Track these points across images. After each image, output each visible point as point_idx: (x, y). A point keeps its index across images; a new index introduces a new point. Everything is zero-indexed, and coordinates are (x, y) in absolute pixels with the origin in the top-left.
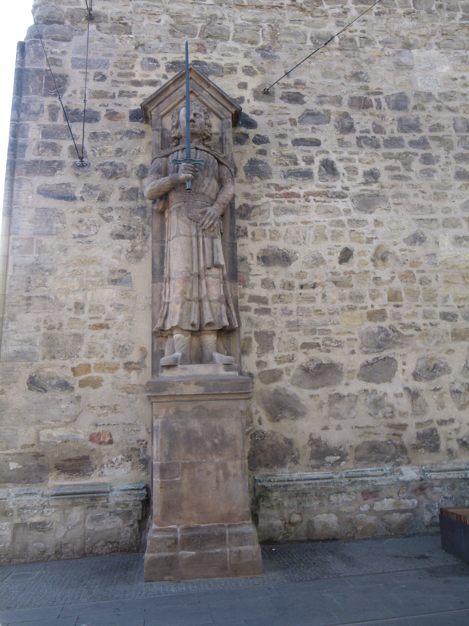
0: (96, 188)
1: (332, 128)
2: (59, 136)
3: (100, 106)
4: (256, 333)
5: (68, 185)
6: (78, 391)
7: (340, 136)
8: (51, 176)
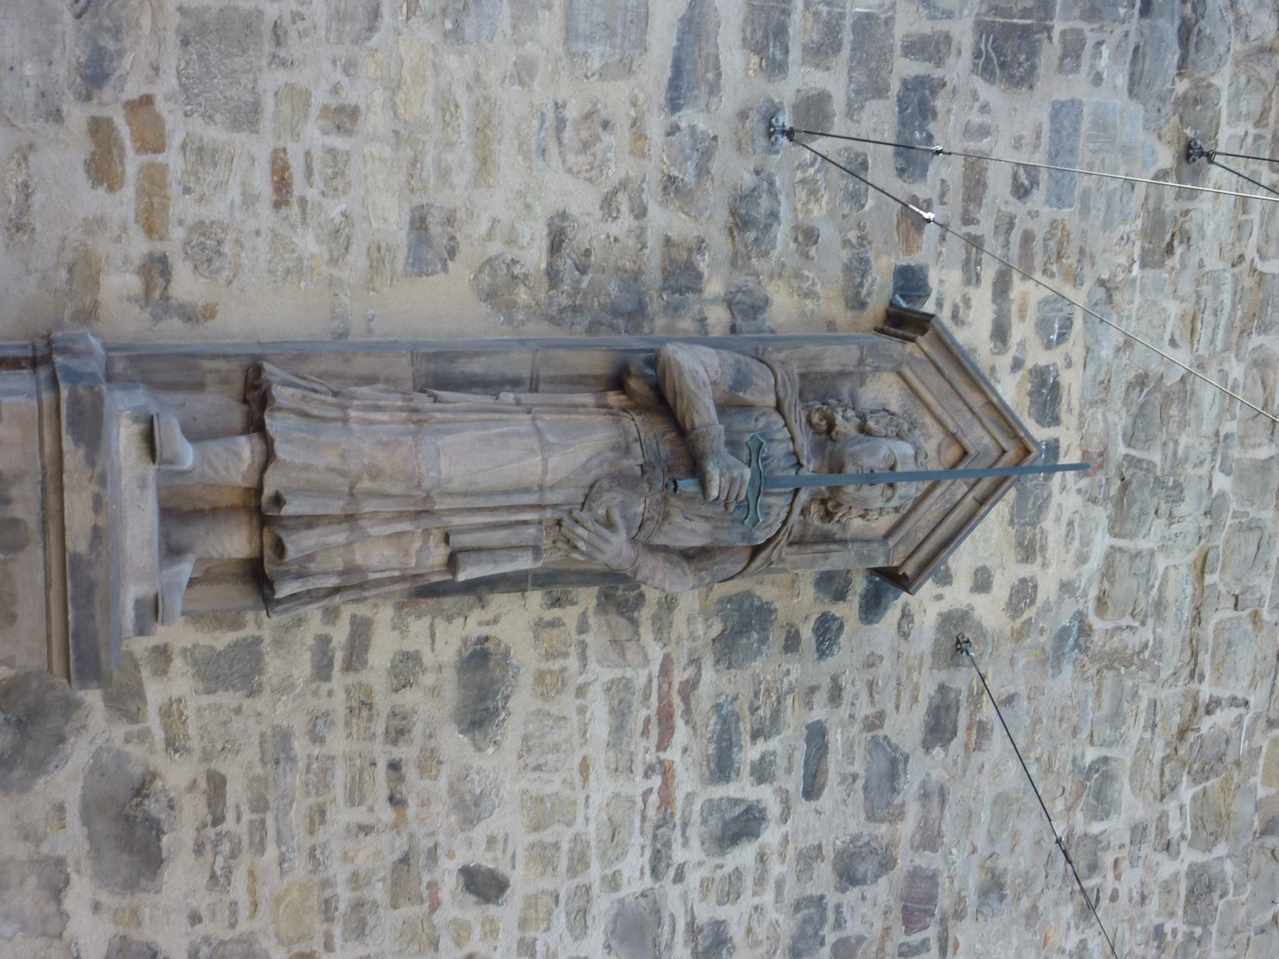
0: (703, 171)
1: (853, 828)
2: (859, 63)
3: (943, 181)
4: (257, 641)
5: (714, 89)
6: (77, 115)
8: (744, 39)
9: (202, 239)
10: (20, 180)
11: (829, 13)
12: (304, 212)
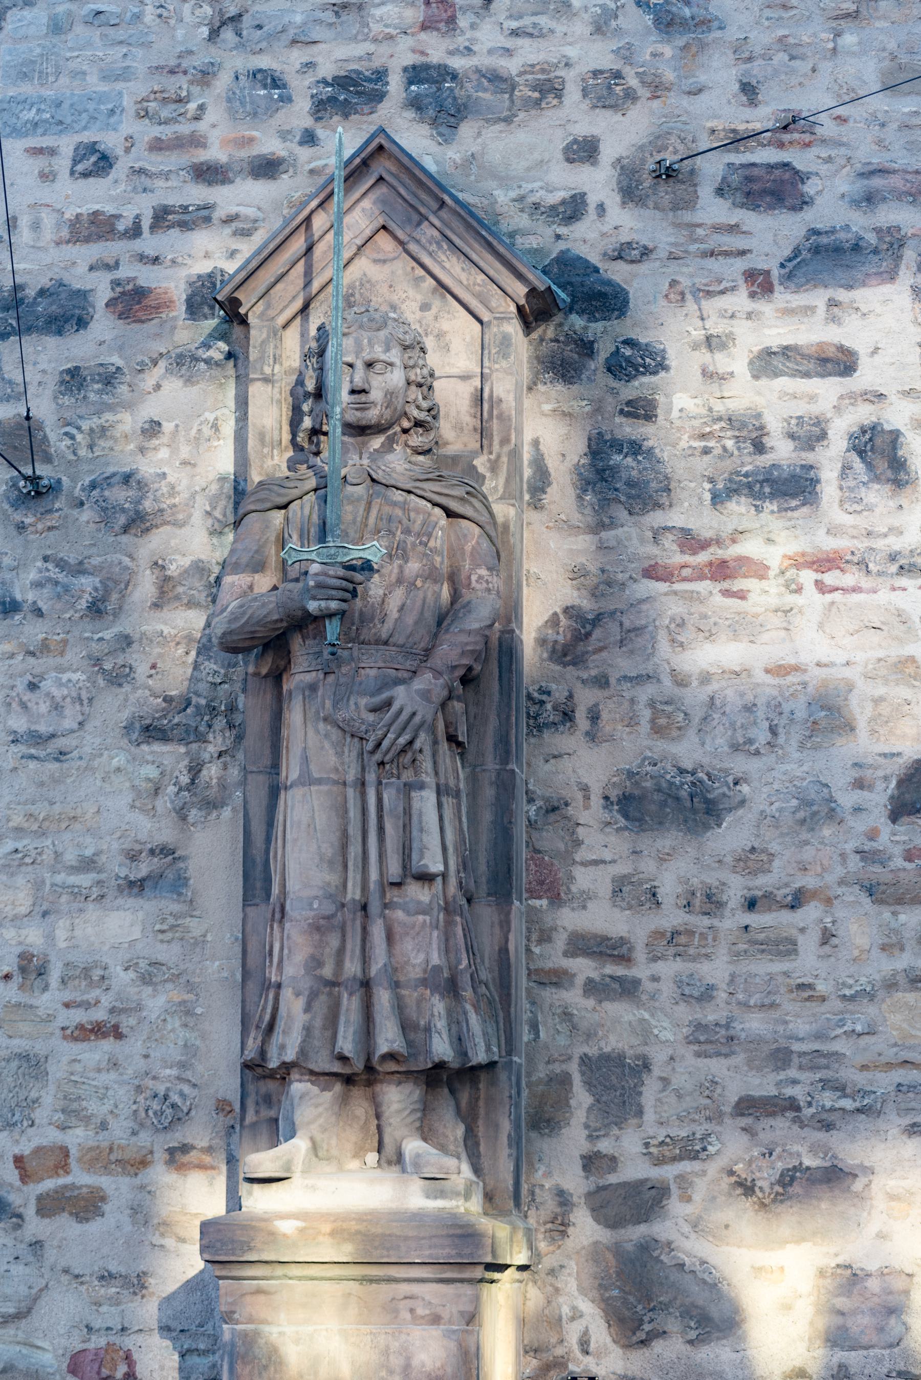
3: (91, 268)
4: (585, 1060)
6: (35, 1226)
9: (151, 1113)
10: (96, 1283)
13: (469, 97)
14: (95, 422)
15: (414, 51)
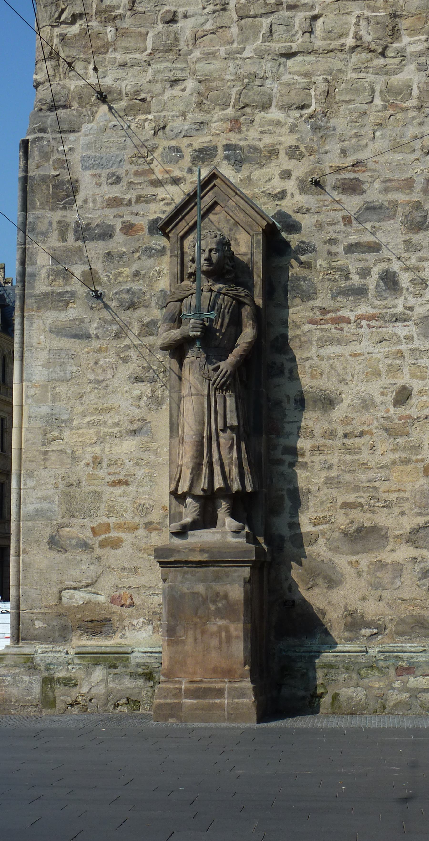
2: (70, 260)
3: (114, 217)
4: (289, 490)
5: (82, 321)
6: (98, 551)
7: (407, 237)
8: (63, 310)
11: (52, 276)
12: (129, 475)
13: (246, 156)
14: (116, 271)
15: (226, 139)
